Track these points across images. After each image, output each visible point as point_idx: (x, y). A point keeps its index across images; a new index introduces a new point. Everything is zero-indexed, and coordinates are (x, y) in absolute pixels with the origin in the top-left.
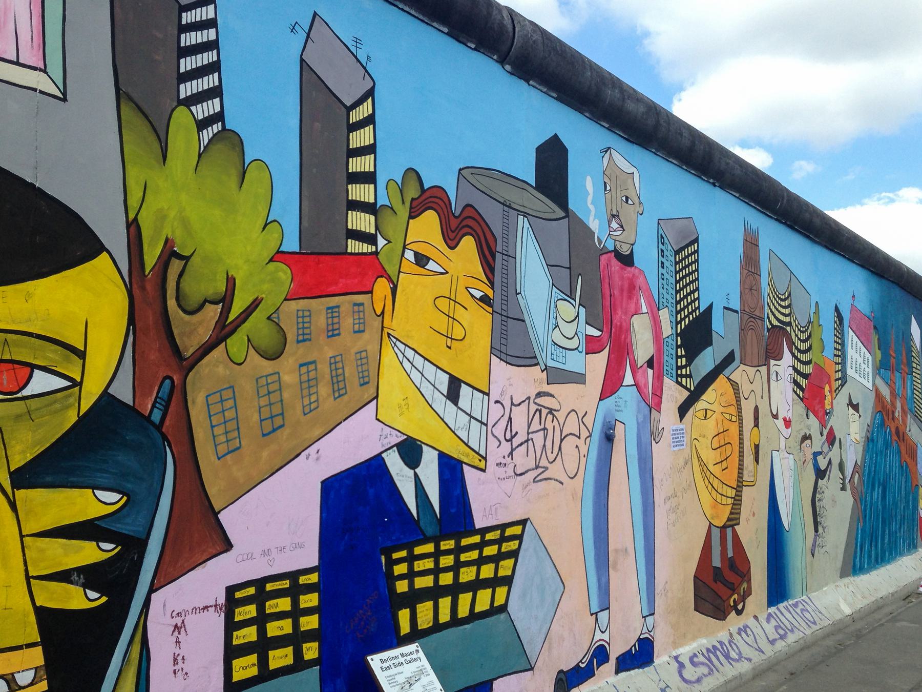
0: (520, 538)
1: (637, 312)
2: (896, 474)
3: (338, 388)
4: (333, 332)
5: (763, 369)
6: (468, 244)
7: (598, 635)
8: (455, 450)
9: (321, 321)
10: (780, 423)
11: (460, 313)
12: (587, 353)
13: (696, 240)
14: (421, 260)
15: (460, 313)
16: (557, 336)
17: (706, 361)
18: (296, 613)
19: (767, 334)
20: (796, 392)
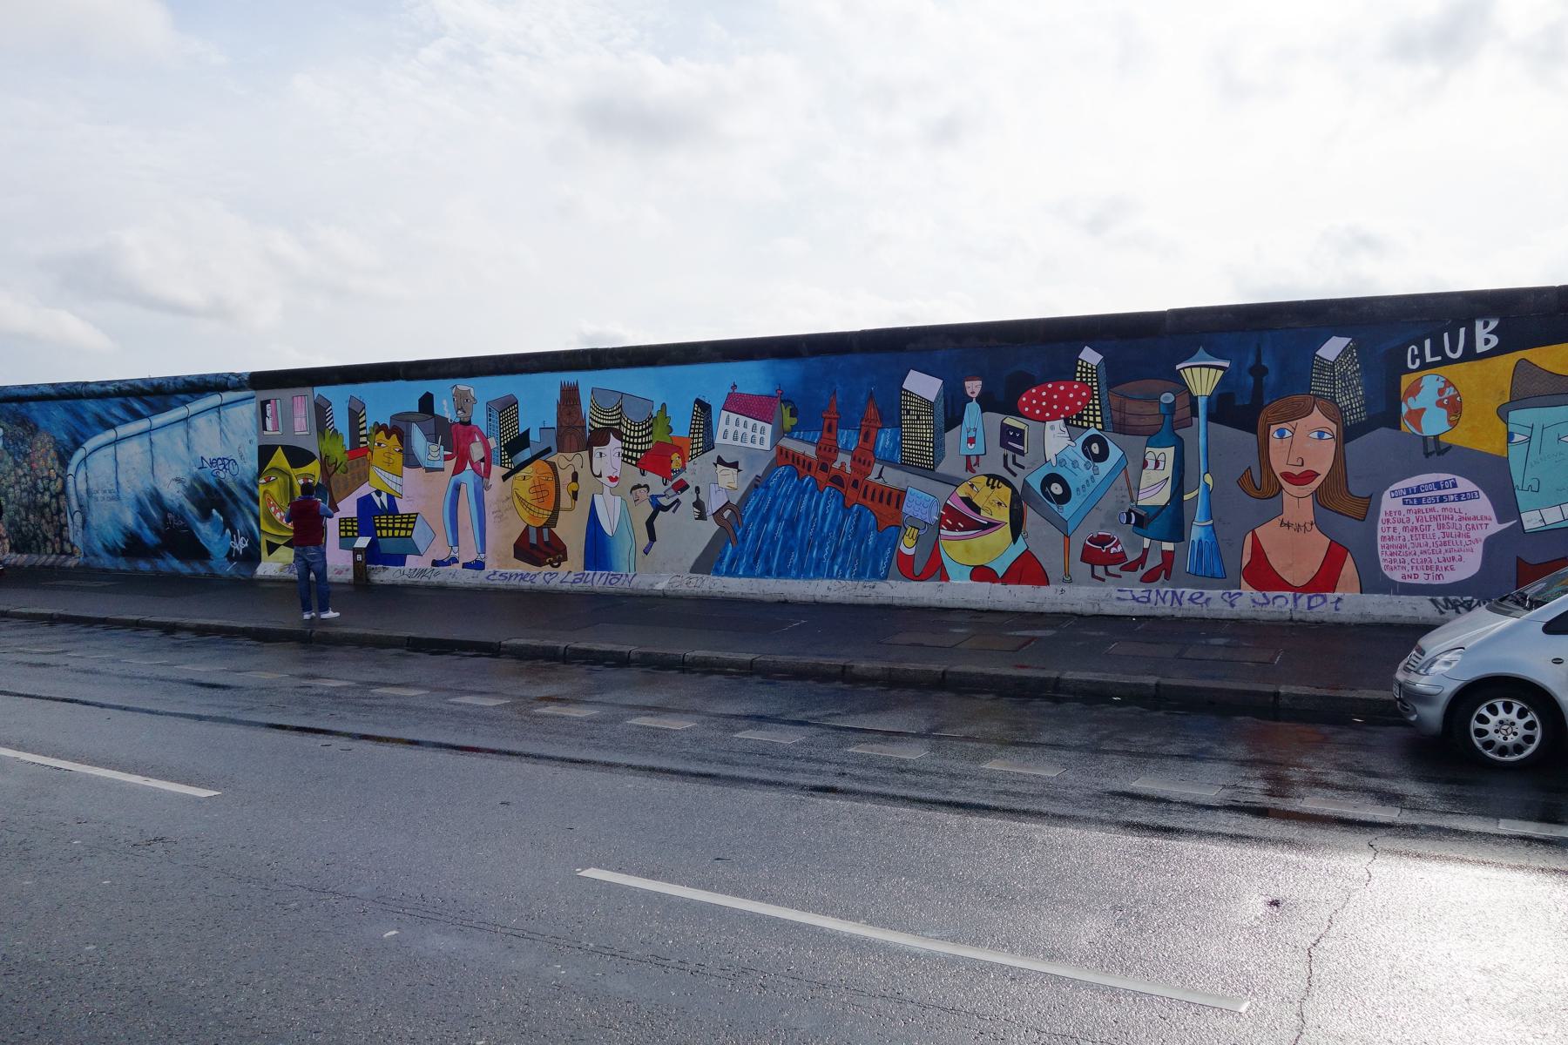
0: (416, 518)
1: (474, 441)
2: (825, 515)
3: (360, 479)
4: (358, 466)
5: (585, 454)
6: (394, 437)
7: (452, 553)
8: (393, 493)
9: (355, 464)
10: (605, 479)
11: (392, 456)
12: (445, 460)
13: (517, 403)
14: (379, 444)
15: (392, 456)
16: (430, 457)
17: (526, 454)
18: (352, 526)
19: (588, 434)
20: (627, 462)
